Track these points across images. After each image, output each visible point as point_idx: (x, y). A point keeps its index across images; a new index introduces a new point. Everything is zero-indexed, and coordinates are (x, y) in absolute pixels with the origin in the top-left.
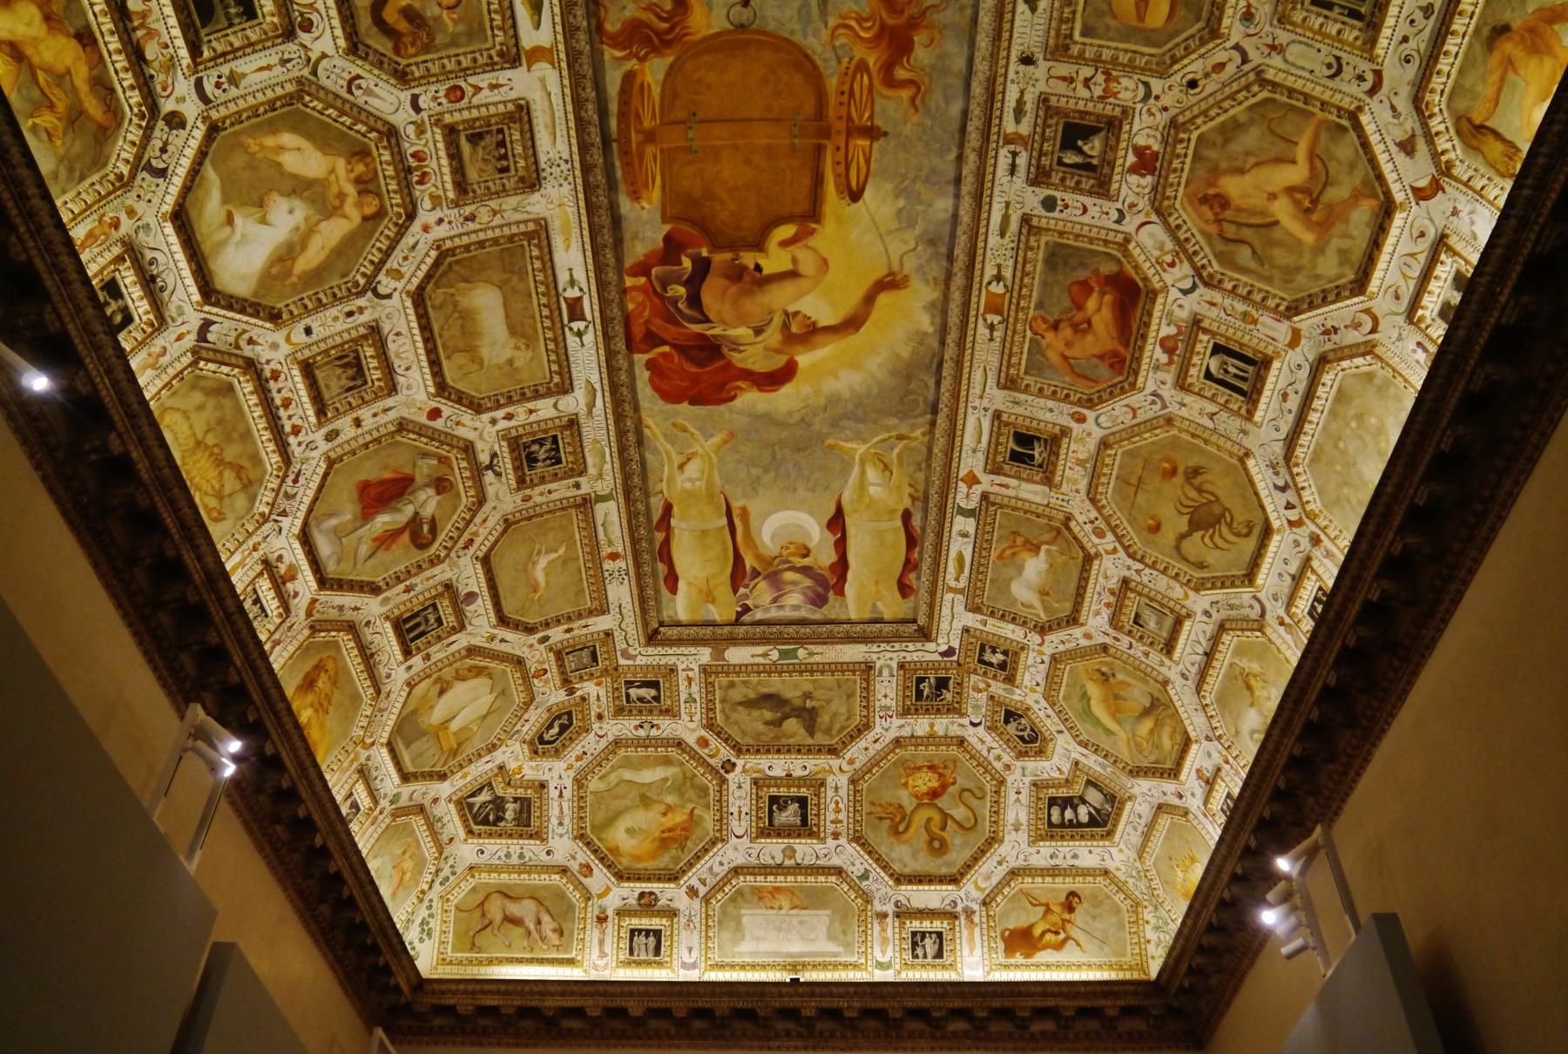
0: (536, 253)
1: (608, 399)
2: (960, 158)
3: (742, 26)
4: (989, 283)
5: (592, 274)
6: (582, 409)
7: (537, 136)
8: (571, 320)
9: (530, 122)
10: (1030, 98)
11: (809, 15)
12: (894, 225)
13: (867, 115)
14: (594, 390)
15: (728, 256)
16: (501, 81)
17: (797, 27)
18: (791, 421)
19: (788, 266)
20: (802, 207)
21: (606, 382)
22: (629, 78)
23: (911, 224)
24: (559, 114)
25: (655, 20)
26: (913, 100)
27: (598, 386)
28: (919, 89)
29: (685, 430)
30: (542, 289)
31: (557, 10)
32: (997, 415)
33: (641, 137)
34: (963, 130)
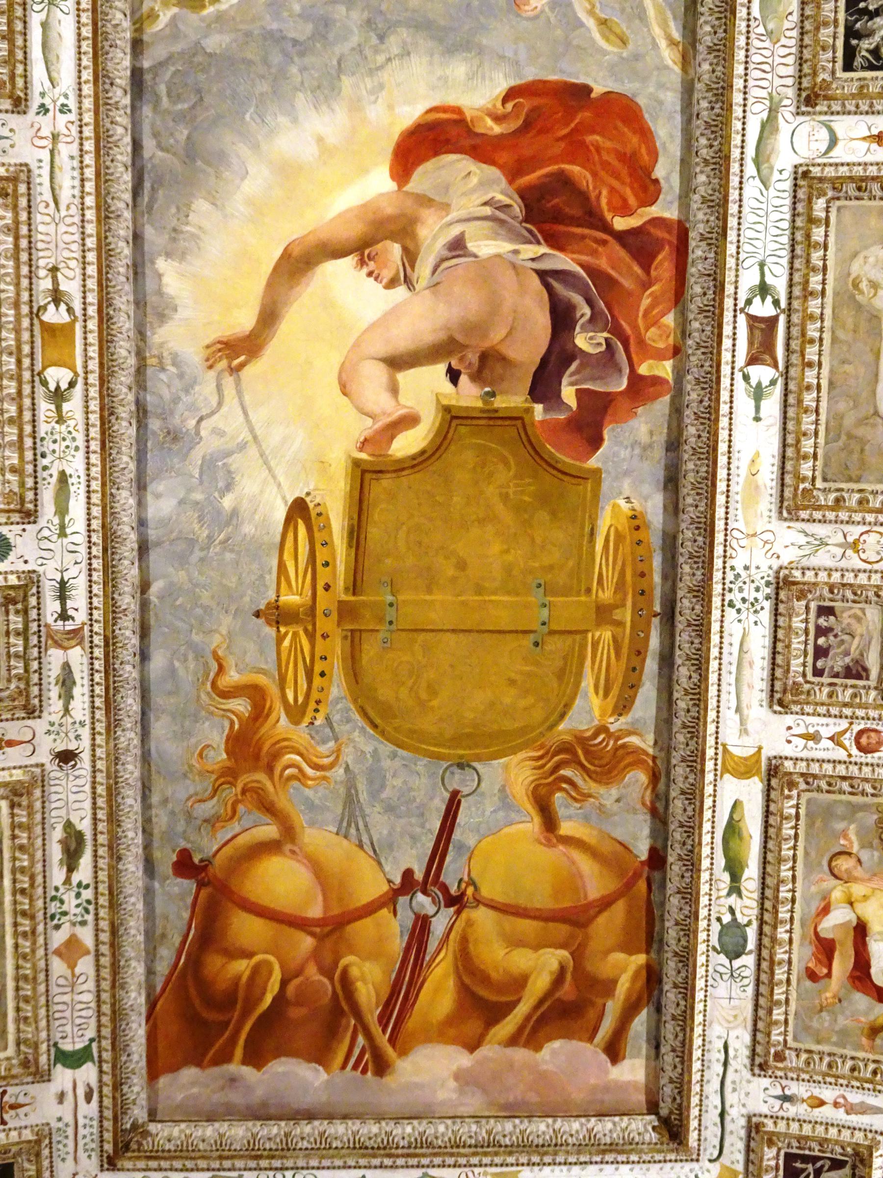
0: (806, 469)
1: (736, 140)
2: (144, 586)
3: (461, 766)
4: (72, 384)
5: (724, 409)
6: (786, 120)
7: (766, 653)
8: (773, 320)
9: (773, 678)
10: (55, 705)
11: (371, 782)
12: (235, 461)
13: (286, 643)
14: (757, 162)
15: (500, 402)
16: (801, 742)
17: (386, 763)
18: (404, 33)
19: (405, 378)
20: (380, 488)
21: (734, 181)
22: (623, 707)
23: (209, 465)
24: (729, 679)
25: (579, 781)
26: (221, 668)
27: (750, 169)
28: (214, 684)
29: (603, 23)
30: (809, 399)
31: (707, 826)
32: (19, 104)
33: (617, 615)
34: (144, 632)
